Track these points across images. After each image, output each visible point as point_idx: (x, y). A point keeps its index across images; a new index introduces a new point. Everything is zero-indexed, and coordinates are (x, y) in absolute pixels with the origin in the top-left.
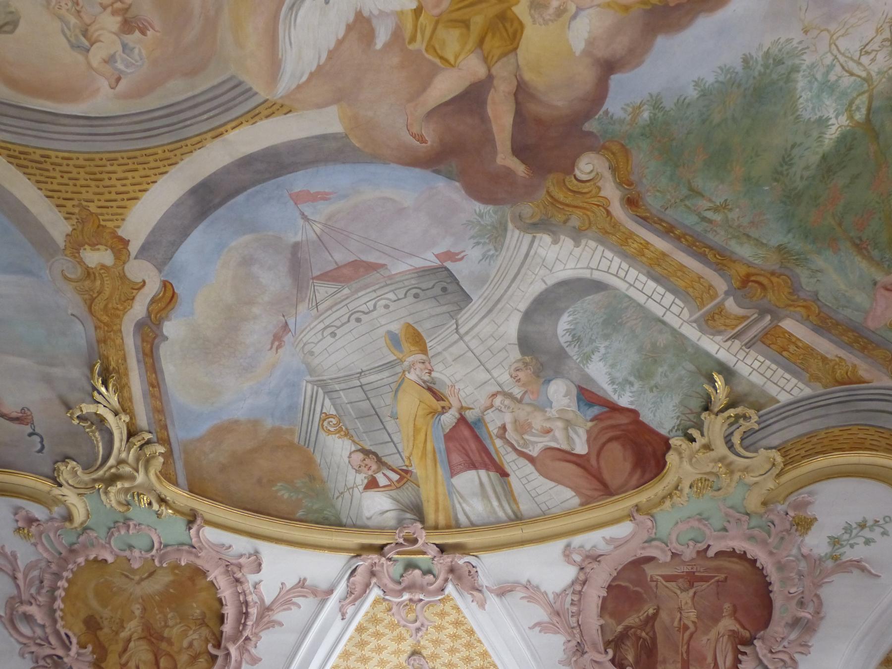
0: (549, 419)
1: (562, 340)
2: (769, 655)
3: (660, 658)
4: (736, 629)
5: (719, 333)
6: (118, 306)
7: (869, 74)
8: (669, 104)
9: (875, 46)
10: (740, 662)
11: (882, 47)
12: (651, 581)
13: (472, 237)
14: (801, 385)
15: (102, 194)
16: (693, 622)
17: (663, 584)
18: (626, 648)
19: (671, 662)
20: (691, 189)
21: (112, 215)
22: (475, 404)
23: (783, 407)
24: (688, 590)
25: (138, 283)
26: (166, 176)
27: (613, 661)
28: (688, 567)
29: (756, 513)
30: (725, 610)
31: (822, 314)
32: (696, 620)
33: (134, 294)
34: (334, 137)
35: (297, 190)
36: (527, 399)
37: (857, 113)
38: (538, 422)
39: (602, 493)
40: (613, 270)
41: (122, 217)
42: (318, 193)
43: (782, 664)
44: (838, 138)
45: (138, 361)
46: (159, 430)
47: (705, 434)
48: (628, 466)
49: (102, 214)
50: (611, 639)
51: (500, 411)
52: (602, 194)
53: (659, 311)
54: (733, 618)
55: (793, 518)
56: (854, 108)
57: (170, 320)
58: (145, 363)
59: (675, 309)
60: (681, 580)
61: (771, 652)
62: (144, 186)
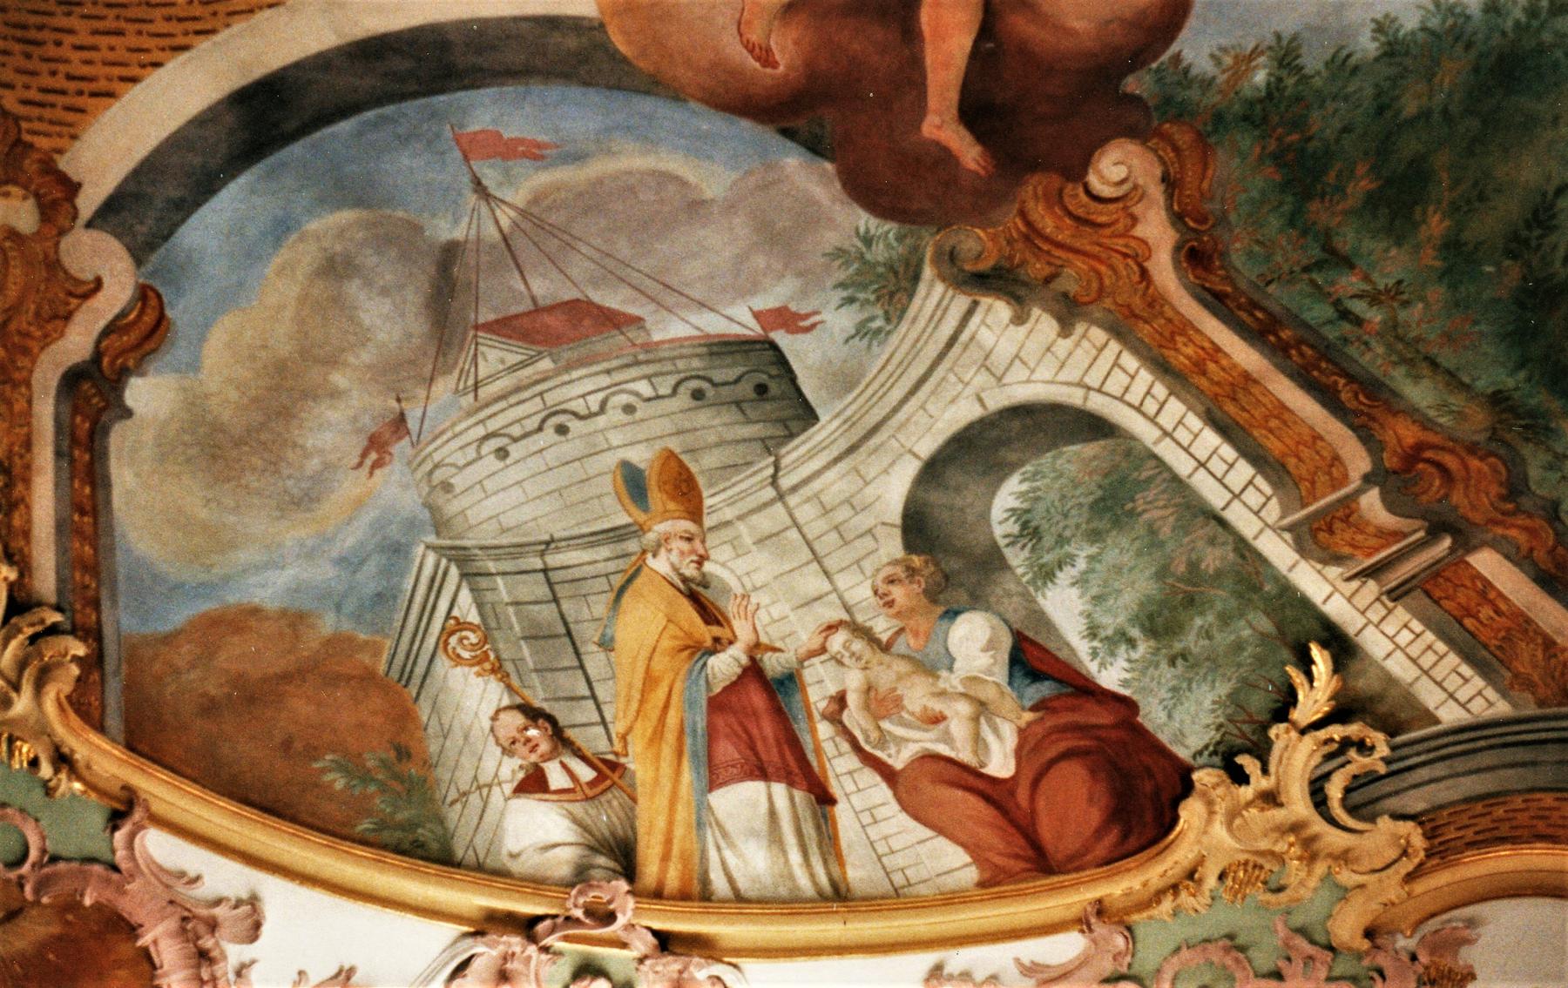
0: (942, 694)
1: (999, 531)
5: (1337, 559)
6: (32, 329)
8: (1313, 60)
13: (842, 285)
14: (1490, 693)
15: (33, 73)
20: (1329, 248)
21: (51, 122)
22: (787, 640)
23: (1446, 733)
25: (83, 283)
26: (184, 56)
29: (1349, 949)
31: (1560, 550)
33: (72, 307)
34: (575, 25)
35: (474, 127)
36: (900, 646)
38: (917, 696)
39: (1028, 866)
40: (1134, 397)
41: (72, 131)
42: (521, 141)
45: (58, 454)
46: (78, 606)
47: (1272, 768)
48: (1095, 816)
49: (28, 119)
51: (840, 663)
52: (1139, 231)
53: (1215, 496)
55: (1427, 968)
57: (142, 375)
58: (72, 461)
59: (1253, 498)
62: (135, 71)
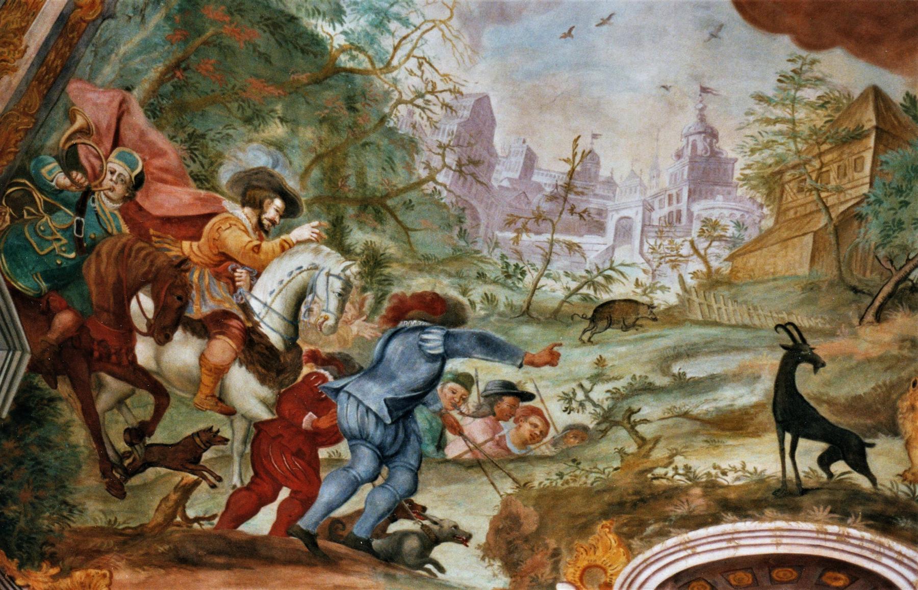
7: (395, 68)
9: (429, 73)
11: (427, 82)
31: (84, 25)
37: (348, 57)
44: (317, 35)
56: (354, 53)
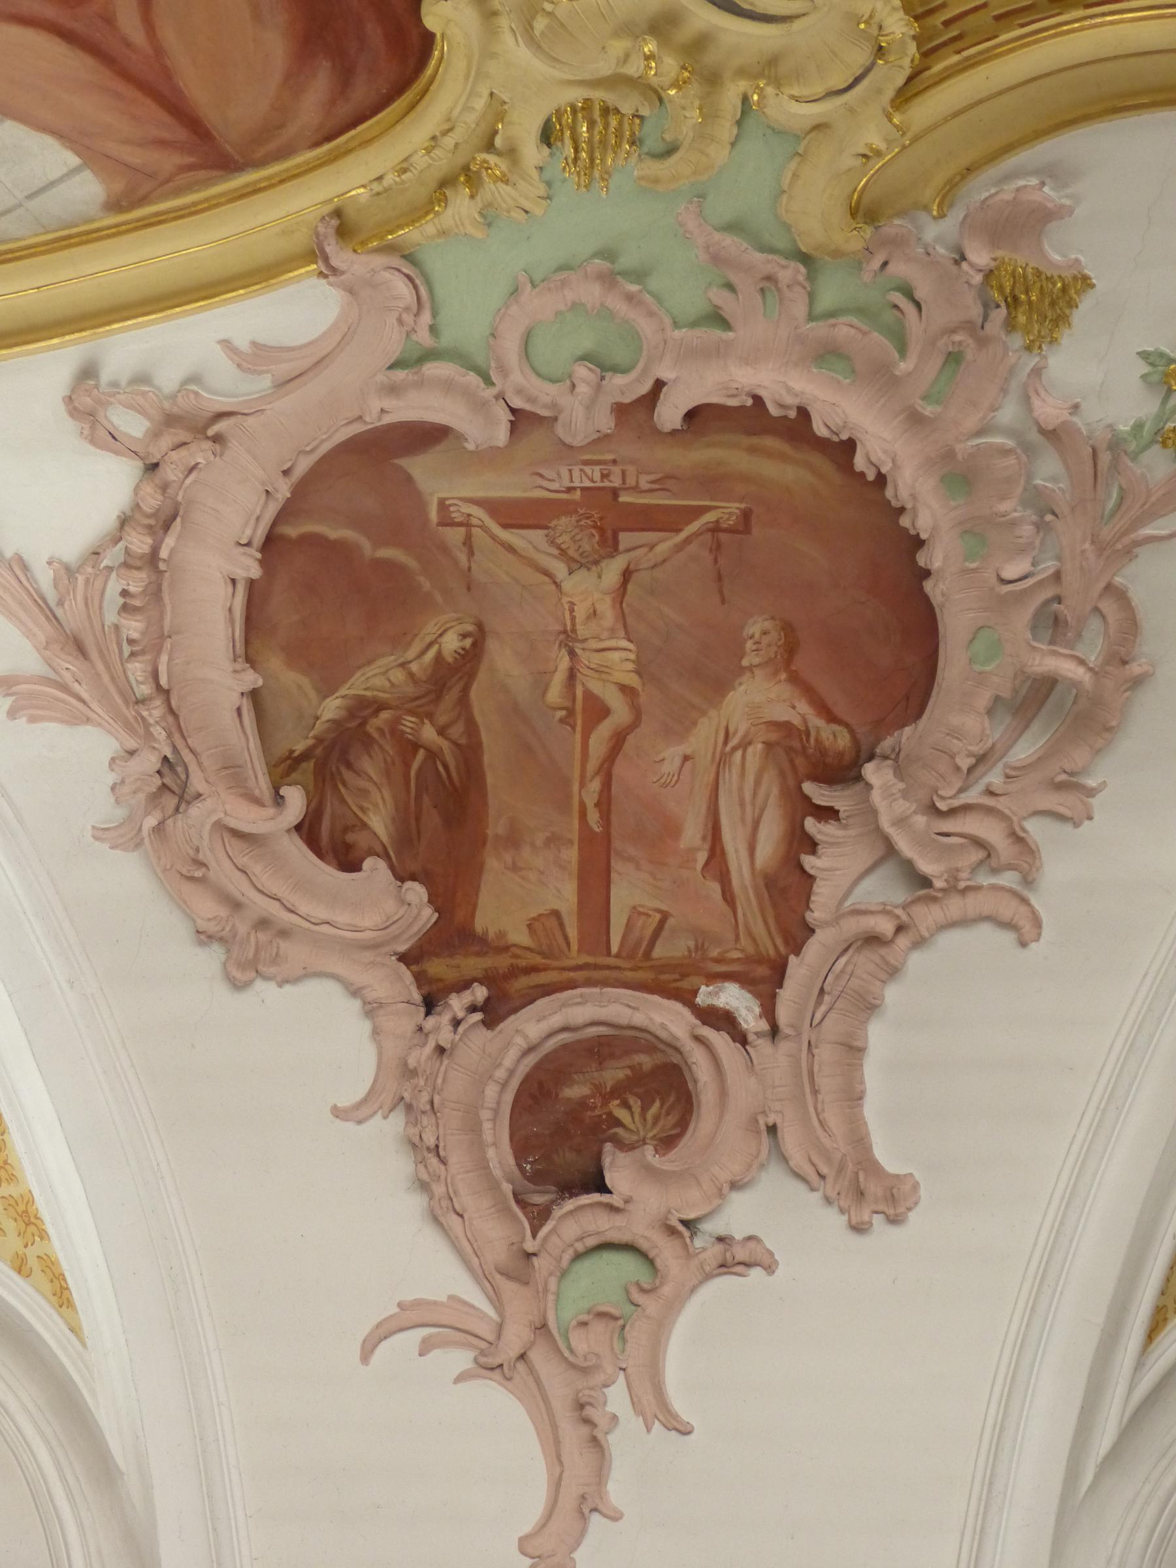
2: (920, 820)
3: (496, 827)
4: (797, 721)
10: (812, 846)
12: (442, 524)
16: (626, 690)
17: (493, 537)
18: (363, 783)
19: (539, 843)
24: (596, 563)
27: (308, 830)
28: (588, 469)
29: (837, 254)
30: (749, 645)
32: (633, 680)
39: (188, 160)
43: (976, 855)
50: (299, 748)
54: (783, 676)
55: (989, 274)
60: (564, 522)
61: (933, 810)
